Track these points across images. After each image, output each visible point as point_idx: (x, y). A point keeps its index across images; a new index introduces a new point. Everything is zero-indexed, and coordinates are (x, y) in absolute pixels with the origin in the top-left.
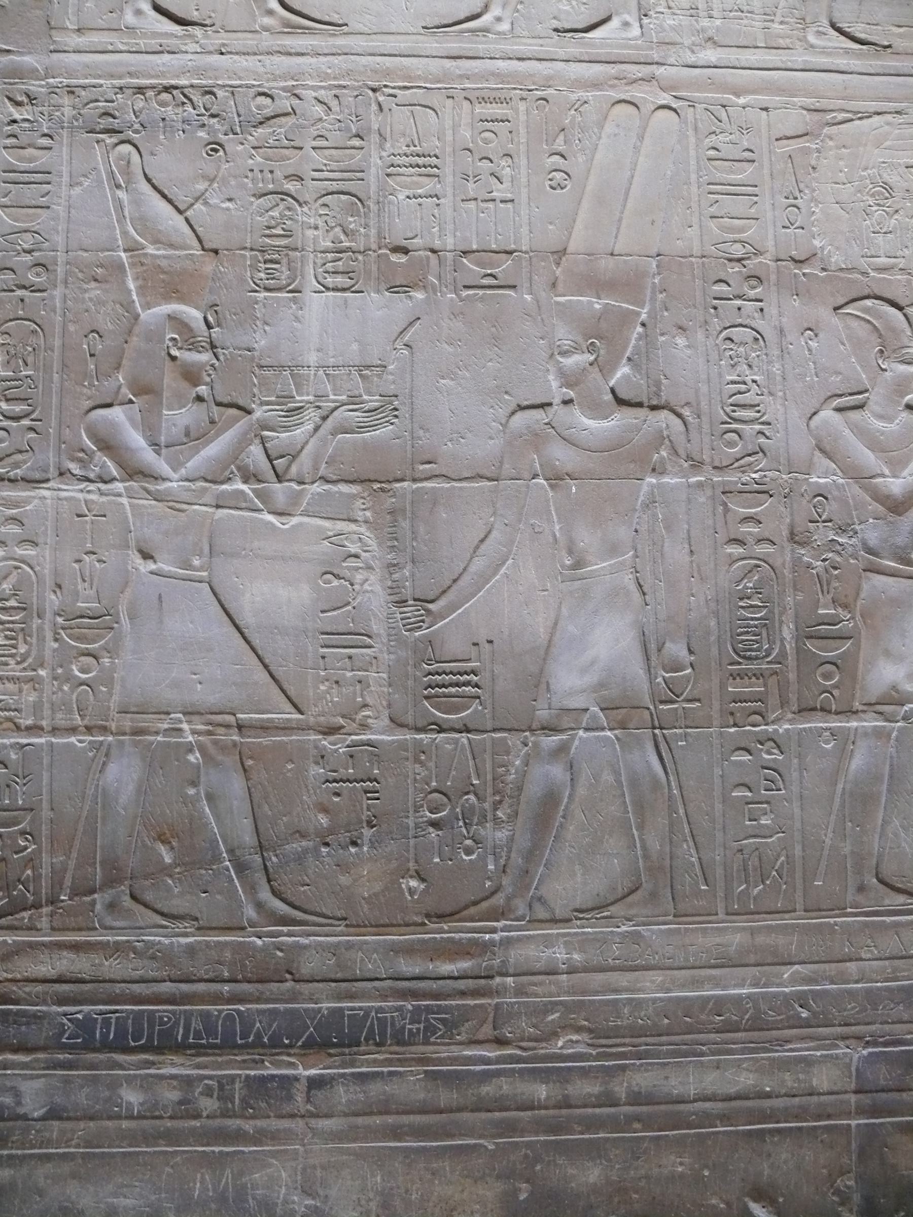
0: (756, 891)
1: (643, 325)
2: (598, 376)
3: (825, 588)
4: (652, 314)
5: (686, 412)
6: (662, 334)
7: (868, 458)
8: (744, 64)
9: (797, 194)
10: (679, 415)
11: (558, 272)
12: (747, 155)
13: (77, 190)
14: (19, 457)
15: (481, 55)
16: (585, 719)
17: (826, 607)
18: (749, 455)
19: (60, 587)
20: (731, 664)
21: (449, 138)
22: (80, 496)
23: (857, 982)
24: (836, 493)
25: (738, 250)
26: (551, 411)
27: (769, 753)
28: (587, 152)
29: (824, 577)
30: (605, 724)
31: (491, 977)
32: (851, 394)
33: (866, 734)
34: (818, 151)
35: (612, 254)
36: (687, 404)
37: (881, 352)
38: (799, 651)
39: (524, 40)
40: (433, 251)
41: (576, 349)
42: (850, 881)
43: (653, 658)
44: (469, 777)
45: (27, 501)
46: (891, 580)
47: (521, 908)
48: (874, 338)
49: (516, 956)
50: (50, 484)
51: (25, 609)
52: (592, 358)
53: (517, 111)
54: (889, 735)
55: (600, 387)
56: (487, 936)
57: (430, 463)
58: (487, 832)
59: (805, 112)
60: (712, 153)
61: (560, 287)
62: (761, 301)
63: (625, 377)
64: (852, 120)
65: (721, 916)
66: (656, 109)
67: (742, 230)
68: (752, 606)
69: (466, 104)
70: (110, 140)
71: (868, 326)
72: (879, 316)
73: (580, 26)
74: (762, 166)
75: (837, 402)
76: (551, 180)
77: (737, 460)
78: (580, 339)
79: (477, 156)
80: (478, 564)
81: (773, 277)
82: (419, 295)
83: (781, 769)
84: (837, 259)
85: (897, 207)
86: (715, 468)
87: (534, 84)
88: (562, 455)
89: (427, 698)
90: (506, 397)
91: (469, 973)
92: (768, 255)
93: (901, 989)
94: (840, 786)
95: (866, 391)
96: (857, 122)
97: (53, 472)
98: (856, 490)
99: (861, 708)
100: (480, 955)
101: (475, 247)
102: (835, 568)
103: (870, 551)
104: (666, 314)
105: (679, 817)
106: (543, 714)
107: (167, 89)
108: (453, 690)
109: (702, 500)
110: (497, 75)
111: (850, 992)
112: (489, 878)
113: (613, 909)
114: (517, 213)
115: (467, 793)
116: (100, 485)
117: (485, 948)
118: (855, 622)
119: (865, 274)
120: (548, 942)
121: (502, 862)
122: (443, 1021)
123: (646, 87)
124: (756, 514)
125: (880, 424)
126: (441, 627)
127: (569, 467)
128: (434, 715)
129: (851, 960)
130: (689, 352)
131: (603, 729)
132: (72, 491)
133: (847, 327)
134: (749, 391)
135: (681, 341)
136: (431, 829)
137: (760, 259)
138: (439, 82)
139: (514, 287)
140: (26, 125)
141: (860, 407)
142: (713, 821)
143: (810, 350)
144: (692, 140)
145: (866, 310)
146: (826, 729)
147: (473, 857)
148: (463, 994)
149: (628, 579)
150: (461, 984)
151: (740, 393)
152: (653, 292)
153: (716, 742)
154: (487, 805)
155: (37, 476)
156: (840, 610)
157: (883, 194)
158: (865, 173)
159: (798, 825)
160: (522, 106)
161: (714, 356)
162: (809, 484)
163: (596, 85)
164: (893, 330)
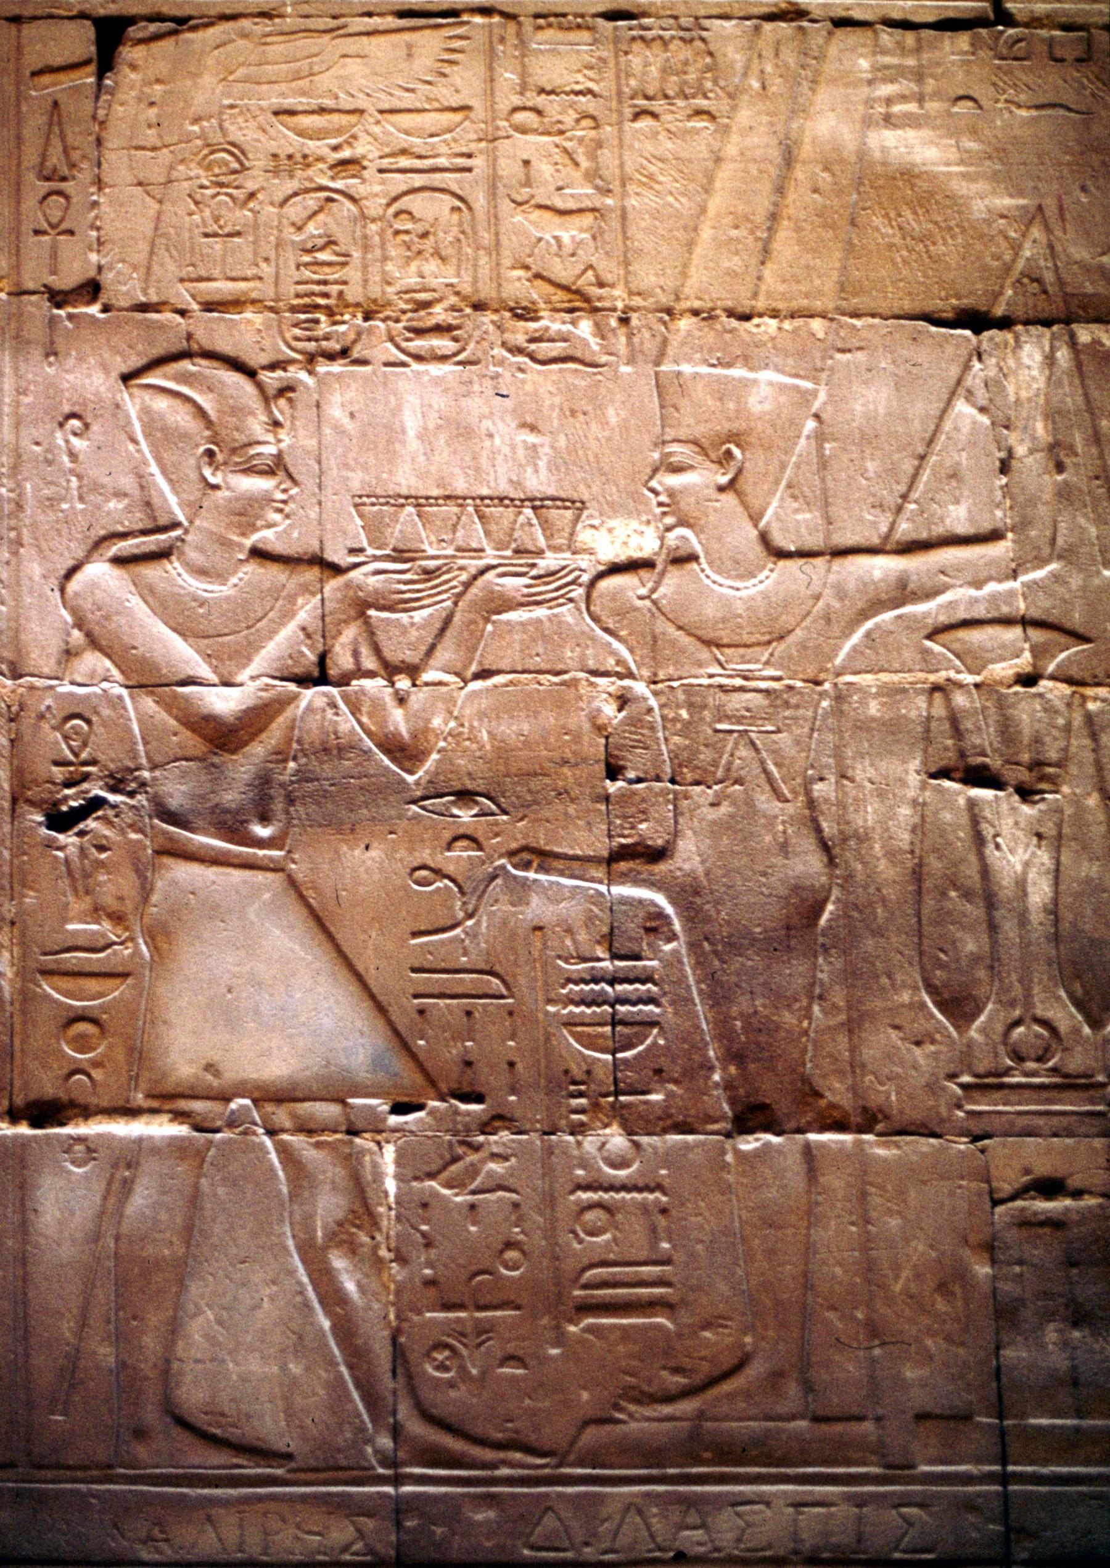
37: (210, 454)
54: (200, 1155)
85: (251, 186)
95: (176, 525)
125: (195, 585)
157: (226, 163)
158: (196, 128)
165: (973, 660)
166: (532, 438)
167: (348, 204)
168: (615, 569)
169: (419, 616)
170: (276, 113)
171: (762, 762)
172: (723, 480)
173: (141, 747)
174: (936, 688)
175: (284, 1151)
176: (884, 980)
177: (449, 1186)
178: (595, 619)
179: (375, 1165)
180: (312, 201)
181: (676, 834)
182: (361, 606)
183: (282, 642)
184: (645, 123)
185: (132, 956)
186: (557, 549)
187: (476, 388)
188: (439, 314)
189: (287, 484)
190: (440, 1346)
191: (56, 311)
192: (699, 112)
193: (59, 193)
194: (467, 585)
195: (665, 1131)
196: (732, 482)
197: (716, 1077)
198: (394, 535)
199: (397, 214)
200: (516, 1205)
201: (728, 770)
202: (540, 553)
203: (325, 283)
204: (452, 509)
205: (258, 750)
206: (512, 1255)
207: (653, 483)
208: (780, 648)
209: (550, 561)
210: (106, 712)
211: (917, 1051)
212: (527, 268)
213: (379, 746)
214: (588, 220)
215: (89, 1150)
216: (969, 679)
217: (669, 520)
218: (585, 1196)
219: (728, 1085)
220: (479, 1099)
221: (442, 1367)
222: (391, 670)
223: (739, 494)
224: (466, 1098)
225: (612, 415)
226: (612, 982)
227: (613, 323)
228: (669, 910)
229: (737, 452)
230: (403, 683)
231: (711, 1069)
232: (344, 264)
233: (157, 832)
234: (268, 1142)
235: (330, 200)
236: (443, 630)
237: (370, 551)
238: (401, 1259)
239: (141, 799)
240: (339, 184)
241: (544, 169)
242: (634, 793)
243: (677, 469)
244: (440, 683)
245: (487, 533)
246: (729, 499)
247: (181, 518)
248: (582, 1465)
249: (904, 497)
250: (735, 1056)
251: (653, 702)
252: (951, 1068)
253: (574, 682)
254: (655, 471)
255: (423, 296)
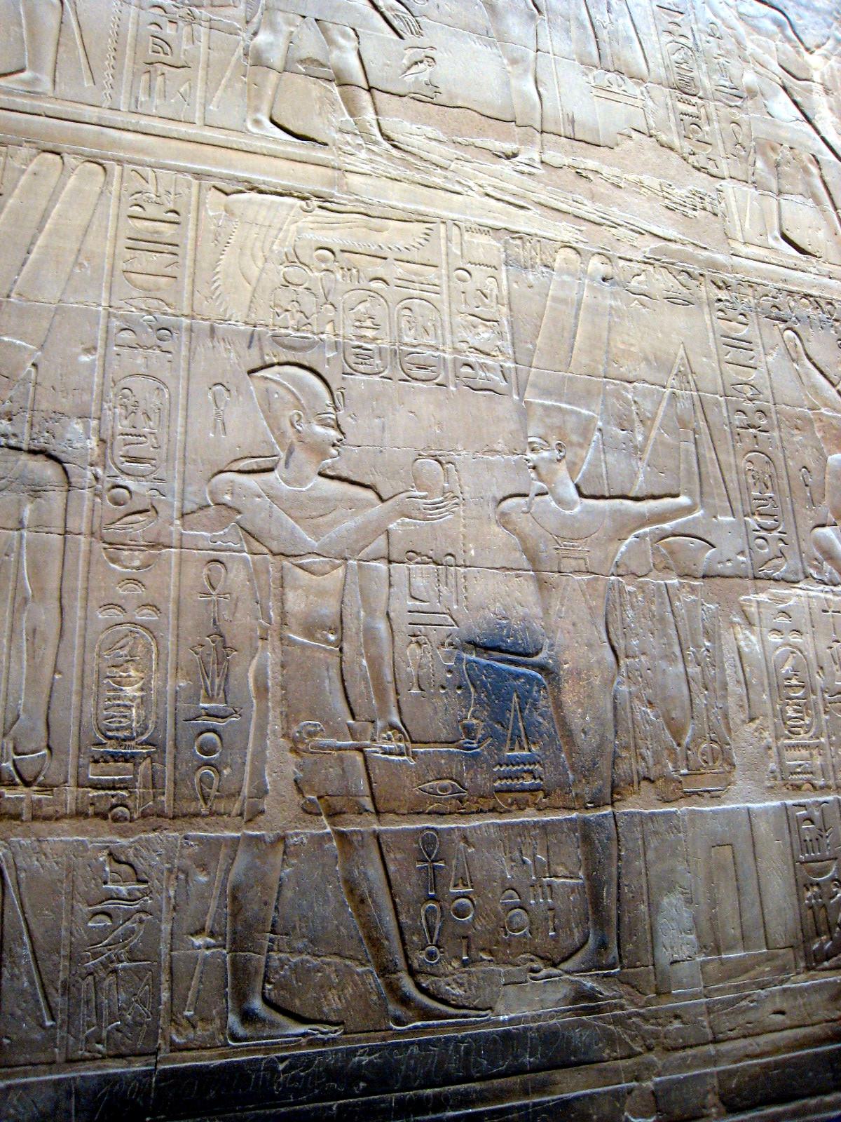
13: (770, 359)
14: (776, 561)
19: (822, 668)
22: (822, 595)
45: (789, 597)
50: (800, 585)
51: (803, 687)
70: (782, 326)
97: (801, 576)
107: (806, 296)
116: (832, 587)
132: (817, 591)
140: (728, 304)
155: (792, 578)
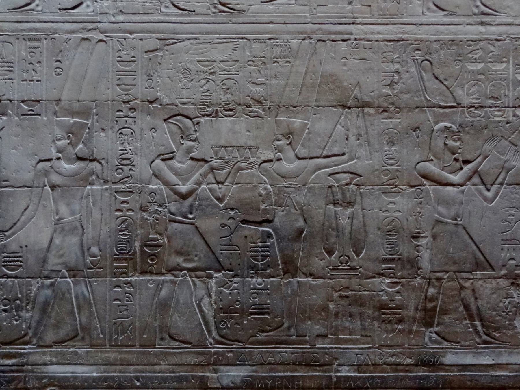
0: (121, 338)
1: (89, 128)
2: (72, 149)
3: (153, 227)
4: (92, 124)
5: (103, 162)
6: (96, 132)
7: (173, 178)
8: (134, 21)
9: (152, 74)
10: (100, 163)
11: (57, 109)
12: (133, 59)
15: (30, 21)
16: (60, 274)
17: (153, 234)
18: (126, 178)
20: (115, 255)
21: (17, 55)
23: (159, 373)
24: (159, 192)
25: (126, 99)
26: (52, 162)
27: (128, 288)
28: (70, 60)
29: (153, 224)
30: (68, 276)
31: (24, 366)
32: (168, 154)
33: (167, 282)
34: (162, 56)
35: (78, 101)
36: (104, 158)
37: (182, 137)
38: (142, 251)
39: (47, 14)
40: (11, 101)
41: (64, 138)
42: (157, 336)
43: (86, 254)
44: (17, 294)
46: (180, 225)
47: (34, 342)
48: (179, 131)
49: (32, 359)
52: (69, 141)
53: (43, 43)
54: (175, 283)
55: (72, 152)
56: (22, 351)
57: (7, 181)
58: (23, 313)
59: (157, 40)
60: (119, 59)
61: (58, 114)
62: (135, 118)
63: (81, 149)
64: (176, 43)
65: (108, 346)
66: (97, 42)
67: (129, 90)
68: (123, 234)
69: (24, 42)
71: (177, 126)
72: (182, 123)
73: (70, 7)
74: (138, 63)
75: (162, 157)
76: (56, 72)
77: (121, 180)
78: (65, 134)
79: (28, 62)
80: (23, 218)
81: (140, 109)
82: (5, 118)
83: (133, 294)
84: (166, 100)
85: (192, 78)
86: (113, 183)
87: (50, 32)
88: (56, 179)
89: (4, 266)
90: (36, 157)
91: (15, 364)
92: (139, 100)
93: (175, 377)
94: (156, 300)
96: (179, 44)
98: (168, 190)
99: (165, 272)
100: (19, 357)
101: (26, 99)
102: (157, 220)
103: (173, 214)
104: (97, 124)
105: (93, 310)
106: (46, 273)
108: (12, 263)
109: (107, 194)
110: (36, 30)
111: (156, 377)
112: (23, 330)
113: (68, 343)
114: (42, 85)
115: (17, 300)
117: (21, 355)
118: (164, 241)
119: (177, 106)
120: (44, 353)
121: (28, 324)
122: (5, 381)
123: (94, 32)
124: (127, 200)
126: (9, 241)
127: (57, 183)
128: (6, 272)
129: (156, 365)
130: (105, 138)
131: (66, 278)
133: (168, 127)
134: (127, 153)
135: (103, 134)
136: (3, 312)
137: (136, 101)
138: (13, 32)
139: (39, 115)
141: (171, 158)
142: (105, 312)
143: (153, 137)
144: (111, 54)
145: (177, 120)
146: (151, 280)
147: (18, 323)
148: (12, 371)
149: (78, 224)
150: (13, 368)
151: (123, 154)
152: (93, 115)
153: (108, 283)
154: (23, 304)
156: (158, 236)
158: (180, 65)
159: (138, 314)
160: (45, 42)
161: (115, 140)
162: (149, 189)
163: (74, 32)
164: (187, 128)
165: (338, 181)
166: (249, 134)
167: (212, 82)
168: (265, 162)
169: (224, 171)
170: (198, 61)
171: (293, 202)
172: (288, 142)
173: (166, 199)
174: (330, 187)
175: (193, 281)
176: (315, 248)
177: (225, 289)
178: (260, 172)
179: (211, 285)
180: (204, 81)
181: (274, 217)
182: (212, 169)
183: (196, 176)
184: (276, 64)
185: (163, 242)
186: (253, 157)
187: (238, 123)
188: (230, 106)
189: (198, 143)
190: (222, 321)
191: (150, 106)
192: (287, 62)
193: (151, 79)
194: (234, 165)
195: (269, 278)
196: (290, 143)
197: (280, 267)
198: (220, 154)
199: (223, 84)
200: (239, 293)
201: (286, 204)
202: (249, 158)
203: (207, 99)
204: (231, 149)
205: (190, 200)
206: (238, 303)
207: (274, 143)
208: (298, 178)
209: (252, 160)
210: (159, 192)
211: (321, 262)
212: (249, 96)
213: (215, 198)
214: (262, 86)
215: (153, 282)
216: (336, 185)
217: (277, 151)
218: (253, 291)
219: (283, 269)
220: (232, 271)
221: (223, 325)
222: (218, 183)
223: (291, 145)
224: (230, 271)
225: (266, 129)
226: (260, 248)
227: (267, 109)
228: (272, 233)
229: (291, 137)
230: (220, 186)
231: (279, 265)
232: (211, 96)
233: (169, 216)
234: (189, 279)
235: (208, 81)
236: (229, 175)
237: (215, 158)
238: (215, 303)
239: (166, 210)
240: (210, 78)
241: (254, 74)
242: (267, 209)
243: (279, 140)
244: (228, 186)
245: (239, 154)
246: (289, 147)
247: (175, 150)
248: (250, 345)
249: (325, 146)
250: (284, 263)
251: (271, 190)
252: (328, 265)
253: (255, 186)
254: (274, 141)
255: (227, 102)
